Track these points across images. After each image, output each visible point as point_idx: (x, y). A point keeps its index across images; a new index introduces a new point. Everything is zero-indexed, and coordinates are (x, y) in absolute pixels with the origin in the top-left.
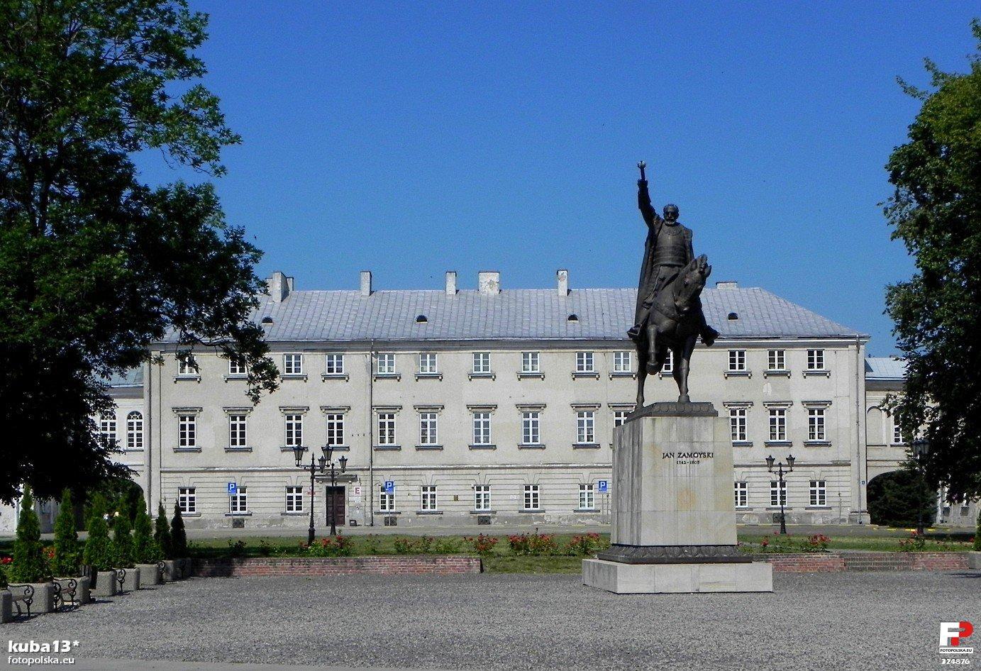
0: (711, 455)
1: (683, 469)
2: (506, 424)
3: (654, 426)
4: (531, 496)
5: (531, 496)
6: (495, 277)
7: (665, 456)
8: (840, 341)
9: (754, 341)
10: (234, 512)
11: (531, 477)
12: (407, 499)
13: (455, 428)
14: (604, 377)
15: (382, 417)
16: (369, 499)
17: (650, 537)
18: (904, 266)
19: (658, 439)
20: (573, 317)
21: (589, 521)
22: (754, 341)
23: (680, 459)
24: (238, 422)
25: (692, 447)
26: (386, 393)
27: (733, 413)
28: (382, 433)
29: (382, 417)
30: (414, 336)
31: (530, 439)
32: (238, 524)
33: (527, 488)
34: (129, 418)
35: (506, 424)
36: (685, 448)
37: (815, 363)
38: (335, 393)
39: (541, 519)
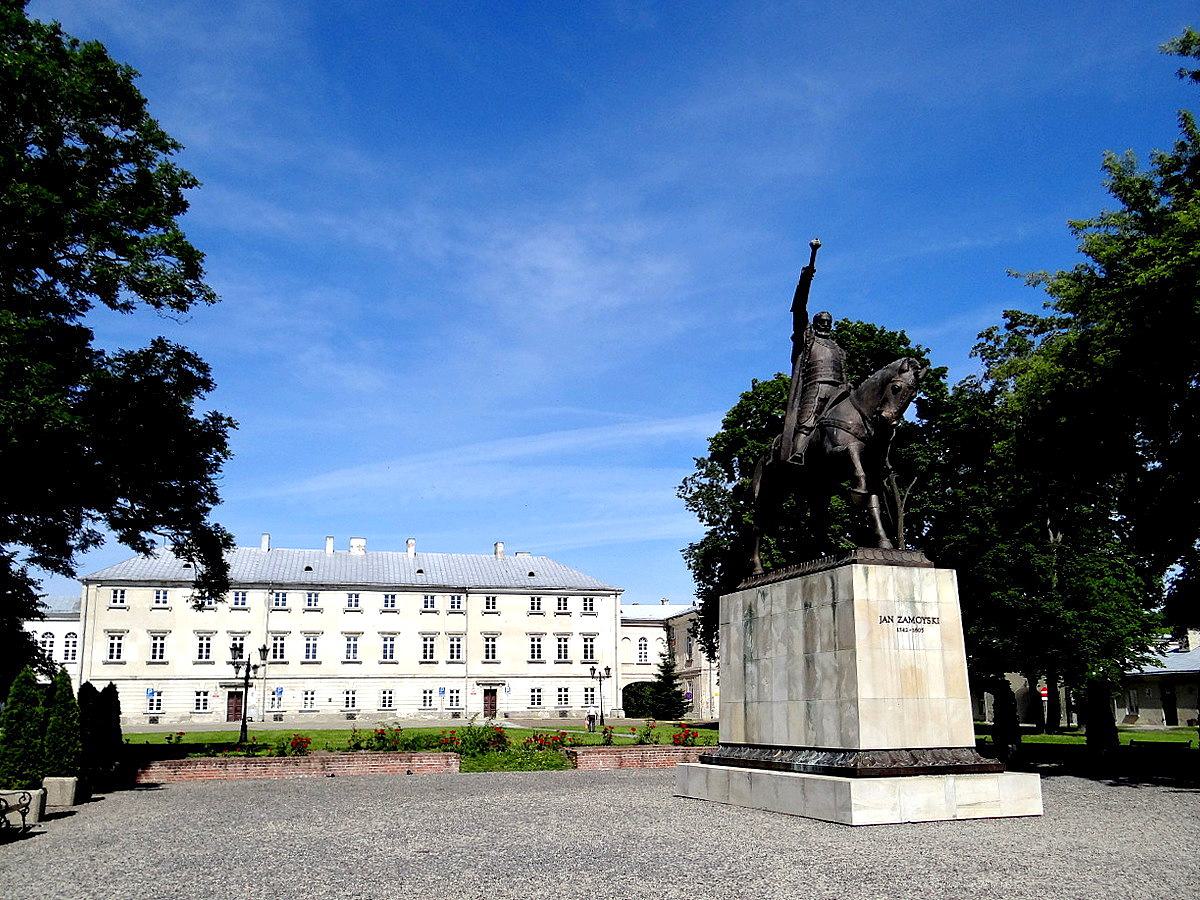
0: (936, 620)
1: (904, 639)
2: (370, 649)
3: (867, 578)
4: (387, 702)
5: (387, 702)
6: (362, 542)
8: (604, 592)
9: (548, 591)
10: (151, 711)
11: (387, 685)
12: (292, 703)
13: (331, 649)
14: (443, 613)
15: (276, 639)
16: (262, 700)
17: (873, 736)
18: (696, 530)
19: (873, 596)
20: (420, 571)
21: (429, 717)
22: (548, 591)
24: (159, 642)
25: (913, 608)
26: (279, 621)
27: (533, 640)
29: (276, 639)
30: (303, 581)
32: (154, 720)
34: (66, 637)
35: (370, 649)
36: (907, 613)
37: (589, 609)
39: (394, 715)
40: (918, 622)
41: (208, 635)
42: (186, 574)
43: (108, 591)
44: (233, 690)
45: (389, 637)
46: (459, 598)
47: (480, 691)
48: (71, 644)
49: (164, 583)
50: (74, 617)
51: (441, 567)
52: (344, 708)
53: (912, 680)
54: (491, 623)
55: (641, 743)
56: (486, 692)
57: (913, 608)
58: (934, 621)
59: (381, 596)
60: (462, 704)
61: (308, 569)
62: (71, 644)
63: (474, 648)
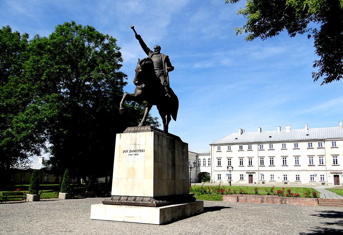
0: (143, 151)
2: (291, 161)
3: (120, 138)
4: (298, 178)
5: (298, 178)
7: (124, 152)
14: (316, 149)
16: (258, 177)
20: (307, 135)
21: (313, 184)
23: (130, 153)
25: (135, 147)
26: (261, 153)
28: (261, 162)
29: (261, 159)
31: (284, 163)
33: (284, 176)
35: (291, 161)
36: (133, 148)
38: (250, 154)
39: (301, 183)
40: (136, 152)
41: (242, 158)
42: (236, 141)
43: (216, 147)
44: (250, 174)
45: (297, 157)
46: (321, 143)
47: (332, 175)
48: (204, 162)
49: (230, 144)
50: (209, 154)
51: (316, 133)
52: (284, 180)
53: (132, 172)
54: (335, 151)
55: (268, 194)
56: (335, 176)
57: (135, 147)
58: (143, 151)
59: (293, 144)
60: (325, 180)
61: (270, 137)
62: (204, 162)
63: (328, 161)
